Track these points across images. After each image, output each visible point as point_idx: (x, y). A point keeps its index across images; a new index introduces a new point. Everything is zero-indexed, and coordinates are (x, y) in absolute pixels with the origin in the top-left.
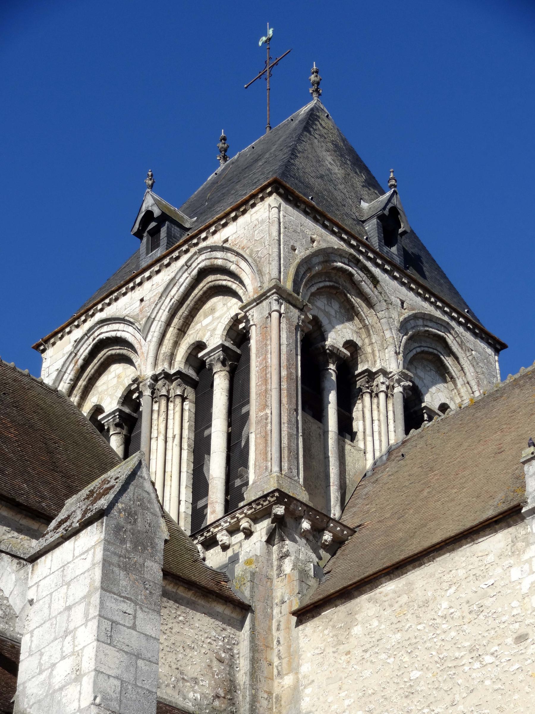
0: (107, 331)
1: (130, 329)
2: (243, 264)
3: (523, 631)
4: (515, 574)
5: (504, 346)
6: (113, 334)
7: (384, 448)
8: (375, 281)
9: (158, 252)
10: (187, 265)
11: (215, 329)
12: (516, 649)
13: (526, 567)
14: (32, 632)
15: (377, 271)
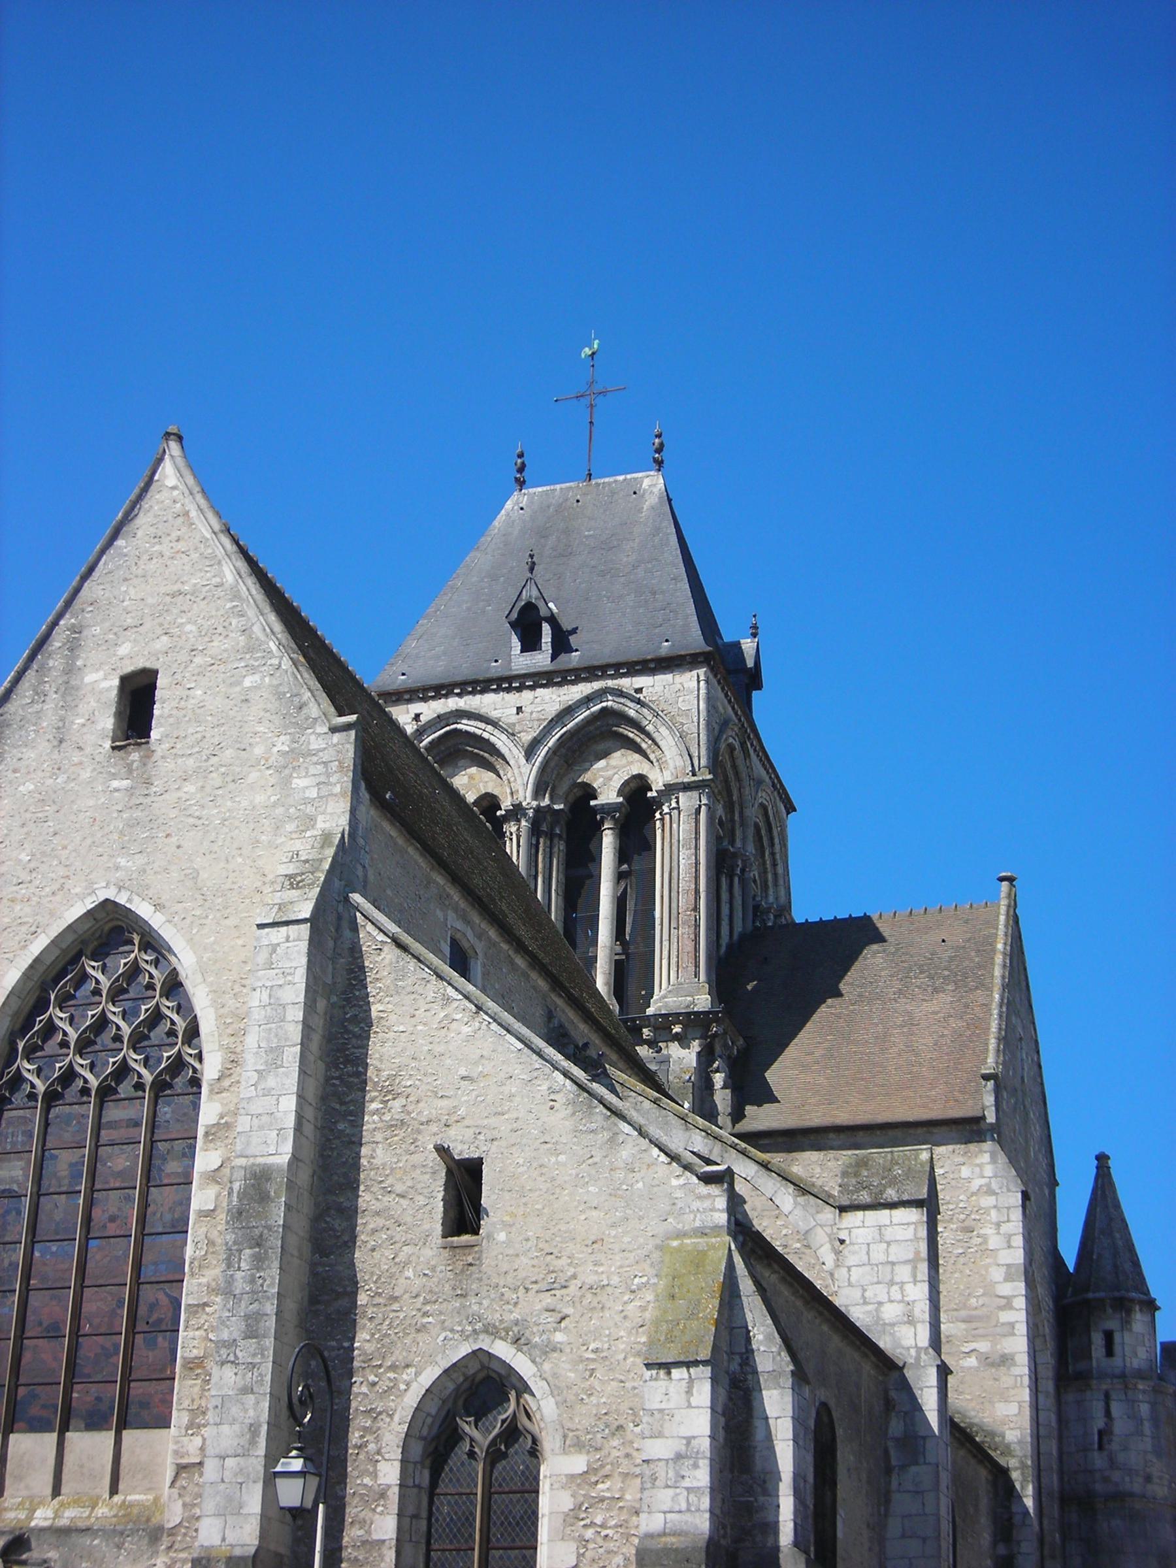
0: (465, 725)
1: (504, 737)
2: (663, 730)
3: (966, 1223)
4: (965, 1172)
5: (795, 810)
6: (479, 732)
7: (736, 936)
8: (747, 755)
9: (541, 659)
10: (588, 700)
11: (610, 779)
12: (960, 1236)
13: (977, 1170)
14: (849, 1269)
15: (751, 751)
